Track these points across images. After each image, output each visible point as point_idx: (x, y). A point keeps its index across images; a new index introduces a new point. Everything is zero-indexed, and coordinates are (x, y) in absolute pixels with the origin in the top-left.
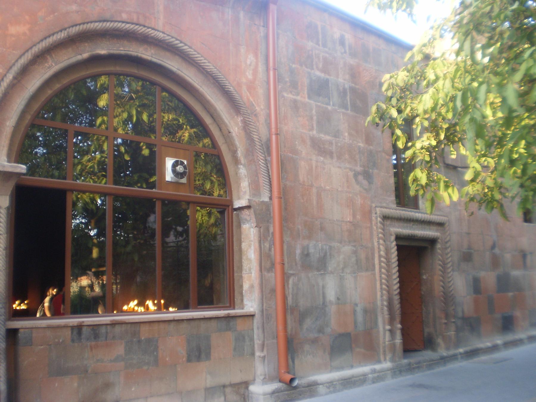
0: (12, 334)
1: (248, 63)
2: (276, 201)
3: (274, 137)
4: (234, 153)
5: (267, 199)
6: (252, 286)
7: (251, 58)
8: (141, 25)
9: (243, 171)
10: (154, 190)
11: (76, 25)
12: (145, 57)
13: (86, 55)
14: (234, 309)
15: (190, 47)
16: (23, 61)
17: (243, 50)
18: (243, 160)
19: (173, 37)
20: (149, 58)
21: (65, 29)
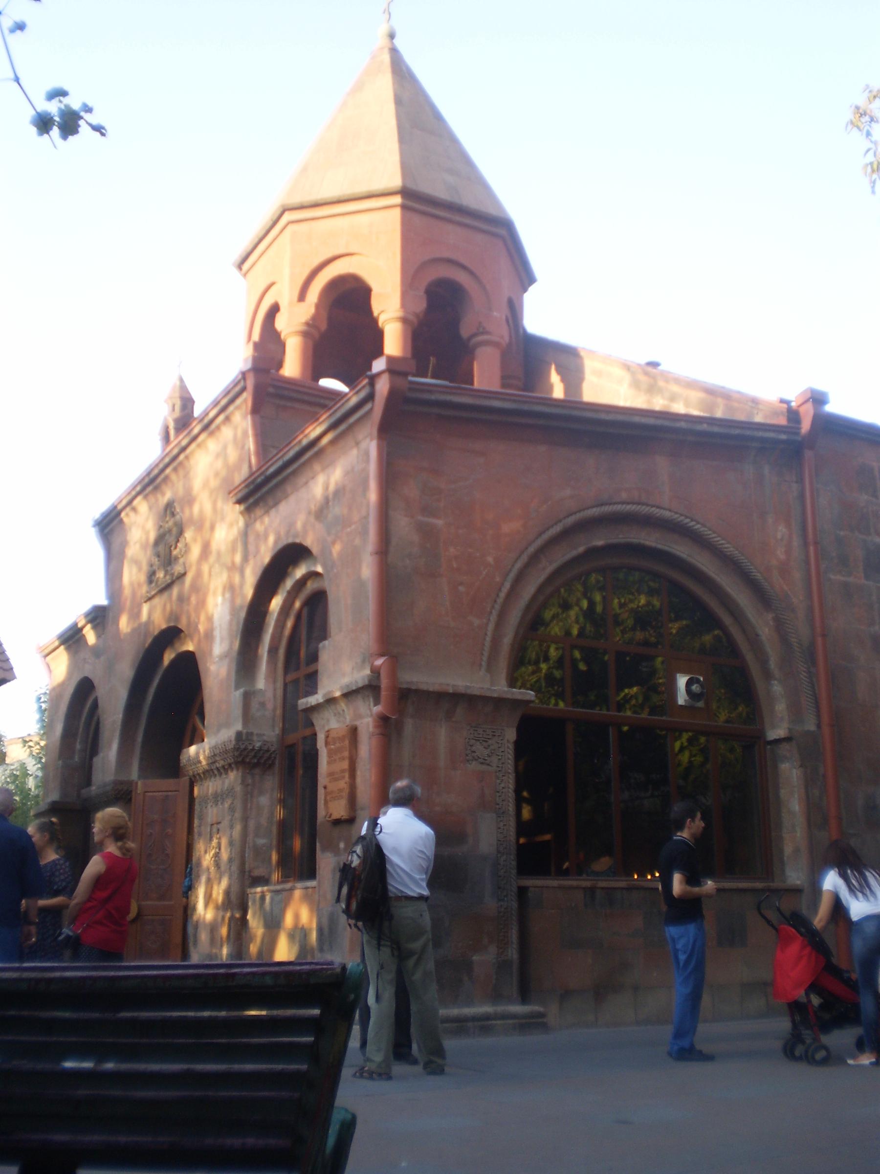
0: (522, 891)
1: (779, 536)
2: (826, 730)
3: (819, 640)
4: (764, 663)
5: (813, 728)
6: (797, 850)
7: (782, 530)
8: (643, 504)
9: (777, 688)
10: (664, 718)
11: (571, 515)
12: (648, 543)
13: (581, 549)
14: (773, 881)
15: (704, 525)
16: (519, 565)
17: (770, 520)
18: (777, 673)
19: (682, 515)
20: (653, 544)
21: (560, 521)
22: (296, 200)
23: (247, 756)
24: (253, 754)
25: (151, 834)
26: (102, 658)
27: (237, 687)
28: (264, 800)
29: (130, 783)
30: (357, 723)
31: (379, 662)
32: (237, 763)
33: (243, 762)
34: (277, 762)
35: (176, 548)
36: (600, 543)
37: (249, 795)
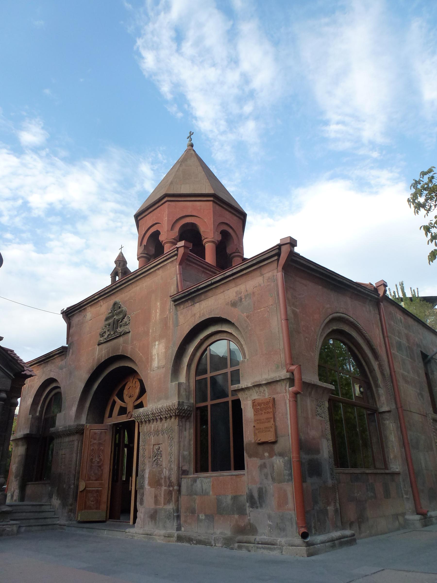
13: (331, 330)
22: (171, 192)
23: (181, 412)
24: (183, 411)
25: (93, 449)
26: (64, 370)
27: (172, 381)
28: (186, 434)
29: (83, 425)
30: (275, 396)
31: (293, 367)
32: (176, 416)
33: (179, 416)
34: (192, 415)
35: (121, 322)
36: (335, 328)
37: (180, 431)
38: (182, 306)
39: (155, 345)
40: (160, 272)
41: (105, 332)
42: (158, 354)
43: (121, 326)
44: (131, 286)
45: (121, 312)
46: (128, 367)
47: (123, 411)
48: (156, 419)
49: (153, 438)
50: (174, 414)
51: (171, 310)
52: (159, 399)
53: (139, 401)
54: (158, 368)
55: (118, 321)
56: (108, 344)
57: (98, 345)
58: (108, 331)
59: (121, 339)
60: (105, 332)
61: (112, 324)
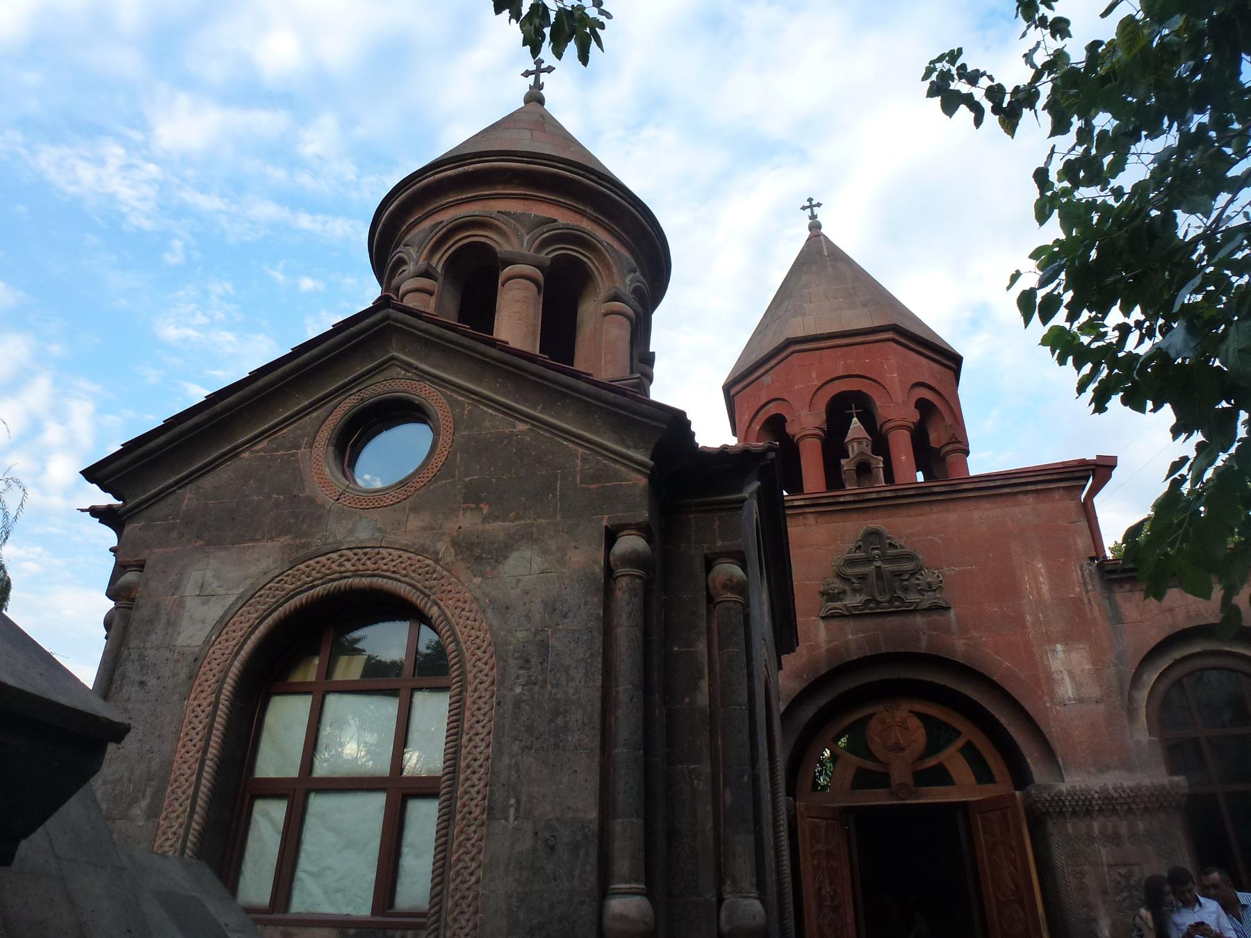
38: (1127, 586)
39: (1054, 651)
40: (1030, 499)
41: (844, 592)
42: (1070, 672)
43: (906, 589)
44: (926, 508)
45: (910, 557)
46: (931, 683)
47: (865, 779)
48: (1114, 809)
49: (1103, 852)
50: (1174, 804)
51: (1090, 587)
52: (1103, 769)
53: (931, 762)
54: (1080, 701)
55: (897, 575)
56: (869, 623)
57: (823, 618)
58: (855, 591)
59: (919, 620)
60: (844, 592)
61: (873, 579)
